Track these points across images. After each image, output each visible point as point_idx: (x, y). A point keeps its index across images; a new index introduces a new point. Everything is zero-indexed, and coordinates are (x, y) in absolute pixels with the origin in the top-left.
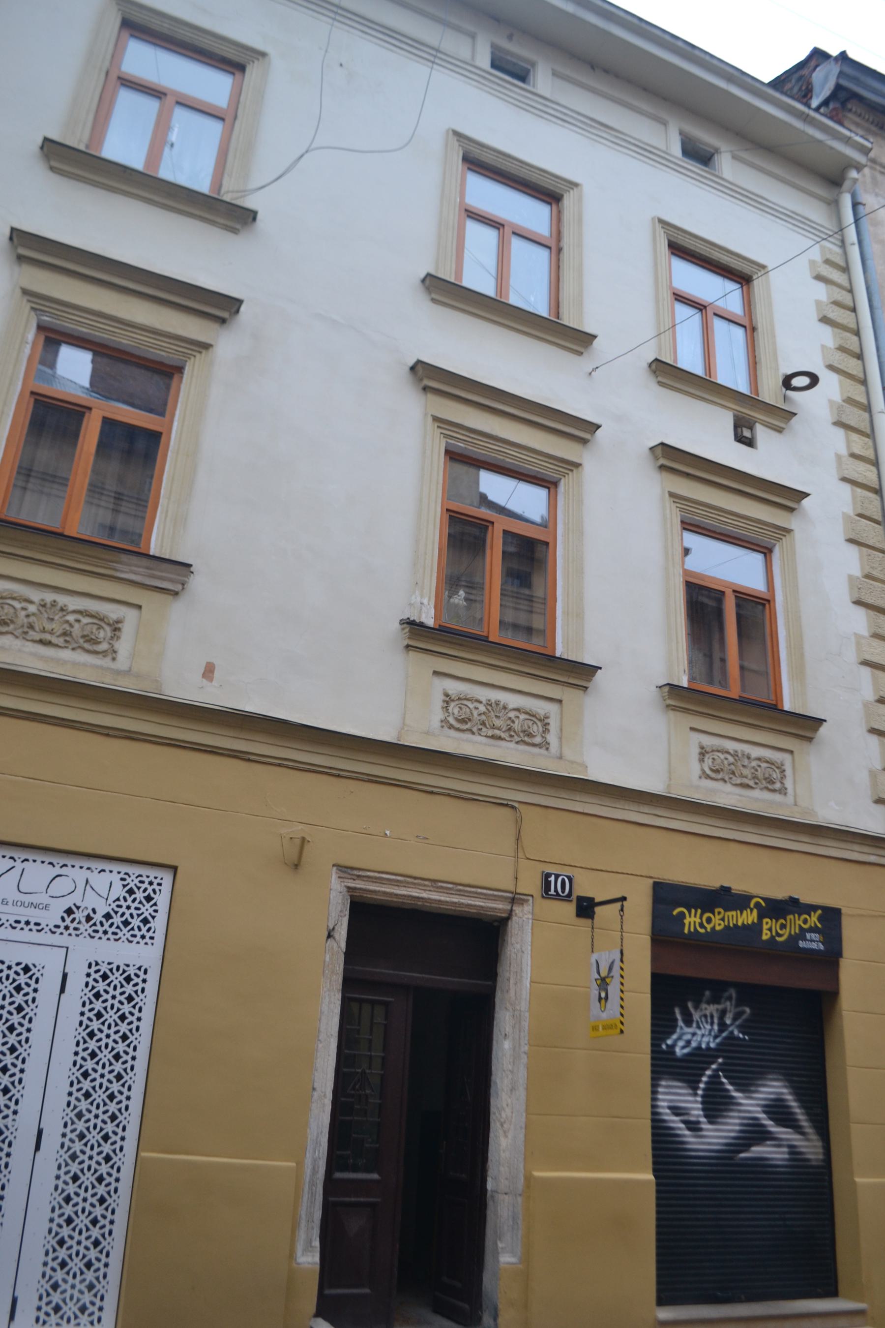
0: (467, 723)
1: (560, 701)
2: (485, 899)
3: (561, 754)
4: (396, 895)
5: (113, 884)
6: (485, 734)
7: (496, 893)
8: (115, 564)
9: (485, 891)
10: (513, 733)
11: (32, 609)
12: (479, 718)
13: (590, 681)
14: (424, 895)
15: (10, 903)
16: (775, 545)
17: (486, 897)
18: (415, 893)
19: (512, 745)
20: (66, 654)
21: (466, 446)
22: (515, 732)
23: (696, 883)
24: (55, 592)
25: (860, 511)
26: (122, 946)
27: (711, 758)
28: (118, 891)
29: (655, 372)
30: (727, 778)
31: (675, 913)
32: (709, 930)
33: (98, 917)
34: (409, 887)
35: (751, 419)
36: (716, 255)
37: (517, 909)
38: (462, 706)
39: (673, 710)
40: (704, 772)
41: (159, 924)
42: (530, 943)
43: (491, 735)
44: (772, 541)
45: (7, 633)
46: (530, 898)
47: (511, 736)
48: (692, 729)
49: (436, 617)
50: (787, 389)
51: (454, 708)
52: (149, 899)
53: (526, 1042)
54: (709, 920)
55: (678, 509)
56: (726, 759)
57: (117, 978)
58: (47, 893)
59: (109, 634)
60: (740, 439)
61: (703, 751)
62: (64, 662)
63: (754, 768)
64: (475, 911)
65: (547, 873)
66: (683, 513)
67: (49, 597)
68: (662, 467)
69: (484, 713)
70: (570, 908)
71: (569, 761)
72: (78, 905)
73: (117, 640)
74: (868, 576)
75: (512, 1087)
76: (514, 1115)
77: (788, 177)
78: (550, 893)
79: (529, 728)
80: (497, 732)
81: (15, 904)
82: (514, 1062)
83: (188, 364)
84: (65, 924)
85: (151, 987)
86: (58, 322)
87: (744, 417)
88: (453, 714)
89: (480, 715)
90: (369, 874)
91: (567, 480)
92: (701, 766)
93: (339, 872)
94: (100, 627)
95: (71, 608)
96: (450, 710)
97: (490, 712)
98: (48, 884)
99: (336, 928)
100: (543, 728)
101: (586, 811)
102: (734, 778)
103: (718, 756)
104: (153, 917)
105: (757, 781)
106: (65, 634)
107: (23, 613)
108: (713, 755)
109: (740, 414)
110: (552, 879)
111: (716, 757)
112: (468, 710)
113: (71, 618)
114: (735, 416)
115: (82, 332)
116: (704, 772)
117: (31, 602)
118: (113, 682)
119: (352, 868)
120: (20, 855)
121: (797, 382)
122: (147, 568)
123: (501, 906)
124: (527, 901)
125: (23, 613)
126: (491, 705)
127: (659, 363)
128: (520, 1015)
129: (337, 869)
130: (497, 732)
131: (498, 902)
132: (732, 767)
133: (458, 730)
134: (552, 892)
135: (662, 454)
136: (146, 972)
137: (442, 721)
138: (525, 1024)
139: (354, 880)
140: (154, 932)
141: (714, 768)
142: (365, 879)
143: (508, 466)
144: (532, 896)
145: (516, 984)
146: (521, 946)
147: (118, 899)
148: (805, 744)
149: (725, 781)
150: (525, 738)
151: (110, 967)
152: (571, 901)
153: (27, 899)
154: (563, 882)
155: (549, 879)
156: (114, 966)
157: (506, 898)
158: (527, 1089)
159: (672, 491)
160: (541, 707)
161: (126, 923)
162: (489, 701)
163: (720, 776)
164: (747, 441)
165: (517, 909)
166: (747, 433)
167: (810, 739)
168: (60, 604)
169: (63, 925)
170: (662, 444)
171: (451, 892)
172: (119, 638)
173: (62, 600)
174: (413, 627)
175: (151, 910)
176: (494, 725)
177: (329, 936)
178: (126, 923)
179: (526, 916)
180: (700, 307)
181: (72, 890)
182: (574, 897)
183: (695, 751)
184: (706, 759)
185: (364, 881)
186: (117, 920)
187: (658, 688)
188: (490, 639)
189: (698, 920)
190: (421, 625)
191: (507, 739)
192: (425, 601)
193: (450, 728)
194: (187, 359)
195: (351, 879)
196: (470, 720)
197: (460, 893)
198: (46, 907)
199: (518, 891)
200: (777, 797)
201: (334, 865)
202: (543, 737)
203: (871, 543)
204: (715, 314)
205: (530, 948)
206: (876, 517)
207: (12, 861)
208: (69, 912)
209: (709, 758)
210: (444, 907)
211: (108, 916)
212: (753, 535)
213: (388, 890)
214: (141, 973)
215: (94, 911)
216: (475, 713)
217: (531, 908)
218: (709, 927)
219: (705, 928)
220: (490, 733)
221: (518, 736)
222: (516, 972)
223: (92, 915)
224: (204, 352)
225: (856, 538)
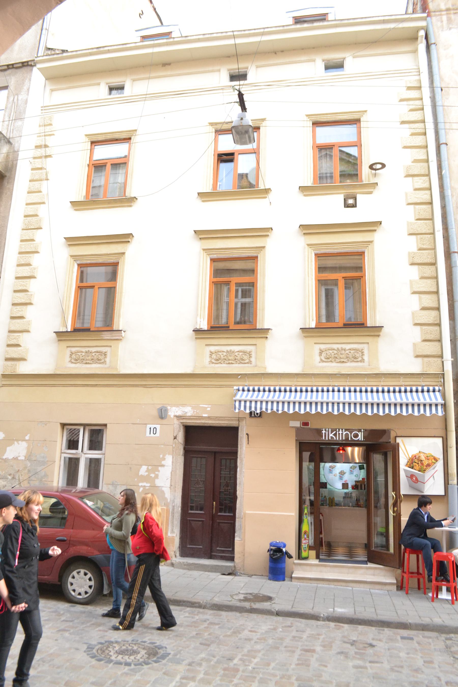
1: (256, 345)
4: (197, 423)
10: (237, 361)
11: (83, 354)
14: (207, 422)
19: (237, 365)
20: (94, 366)
25: (417, 218)
40: (321, 360)
45: (78, 363)
46: (245, 419)
51: (214, 356)
59: (104, 357)
60: (347, 206)
63: (347, 353)
66: (315, 251)
67: (87, 349)
69: (226, 355)
74: (420, 249)
77: (389, 51)
80: (230, 362)
94: (101, 355)
95: (93, 351)
102: (337, 360)
105: (348, 359)
106: (92, 359)
107: (81, 356)
111: (327, 353)
112: (219, 356)
114: (344, 196)
116: (321, 360)
122: (111, 334)
123: (235, 423)
125: (81, 356)
126: (228, 352)
130: (230, 362)
132: (336, 356)
133: (216, 363)
144: (245, 418)
148: (376, 338)
150: (242, 361)
159: (308, 243)
163: (330, 359)
164: (351, 205)
165: (240, 423)
166: (351, 201)
167: (379, 336)
168: (90, 351)
173: (91, 349)
174: (197, 331)
177: (175, 438)
183: (317, 352)
184: (323, 355)
199: (240, 417)
200: (360, 364)
203: (423, 232)
206: (428, 217)
213: (194, 422)
216: (222, 356)
220: (228, 363)
221: (239, 361)
225: (414, 232)
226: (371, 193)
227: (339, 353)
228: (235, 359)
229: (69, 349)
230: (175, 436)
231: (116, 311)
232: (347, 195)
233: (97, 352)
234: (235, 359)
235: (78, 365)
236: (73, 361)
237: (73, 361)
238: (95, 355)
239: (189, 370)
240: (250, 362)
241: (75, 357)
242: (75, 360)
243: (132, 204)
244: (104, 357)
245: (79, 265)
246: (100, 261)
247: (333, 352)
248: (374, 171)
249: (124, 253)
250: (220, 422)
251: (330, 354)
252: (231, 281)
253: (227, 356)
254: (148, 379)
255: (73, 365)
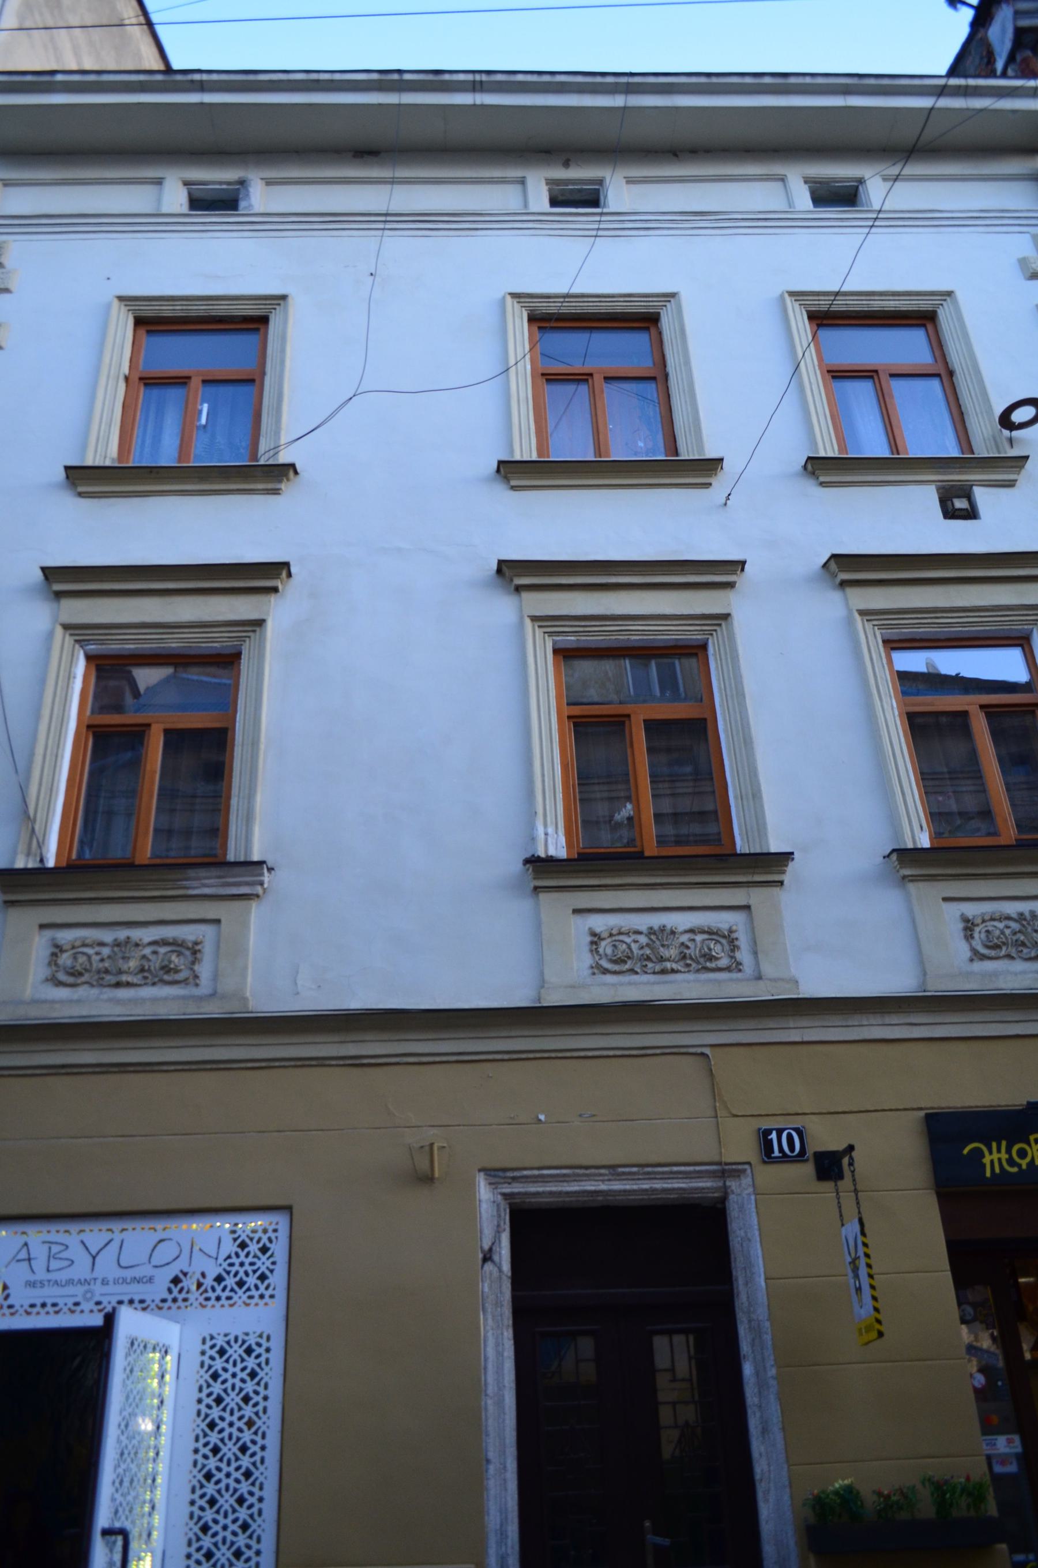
0: (625, 962)
2: (686, 1178)
3: (760, 972)
4: (567, 1193)
5: (222, 1240)
6: (652, 971)
7: (698, 1168)
8: (184, 883)
9: (682, 1168)
10: (689, 962)
11: (106, 951)
12: (641, 952)
13: (784, 872)
14: (603, 1187)
15: (111, 1283)
16: (1032, 630)
17: (687, 1176)
18: (590, 1186)
19: (691, 976)
20: (147, 992)
21: (578, 638)
22: (691, 958)
23: (994, 1104)
24: (129, 928)
26: (239, 1311)
27: (984, 930)
28: (229, 1247)
29: (813, 473)
30: (1013, 952)
31: (965, 1152)
32: (1024, 1167)
33: (209, 1282)
34: (582, 1181)
35: (966, 485)
36: (877, 305)
37: (732, 1184)
38: (614, 943)
39: (912, 881)
40: (975, 952)
41: (278, 1279)
42: (756, 1227)
43: (659, 970)
44: (1026, 627)
46: (747, 1167)
47: (688, 965)
48: (945, 899)
49: (569, 844)
50: (1011, 431)
52: (264, 1250)
53: (773, 1363)
54: (1022, 1154)
55: (876, 628)
56: (1008, 927)
57: (235, 1351)
58: (150, 1262)
60: (950, 513)
61: (970, 925)
62: (143, 1001)
64: (676, 1196)
65: (765, 1129)
67: (122, 934)
68: (844, 584)
69: (648, 945)
70: (808, 1169)
71: (770, 980)
72: (185, 1270)
73: (199, 963)
75: (763, 1428)
76: (772, 1468)
78: (773, 1155)
79: (710, 949)
81: (116, 1282)
82: (760, 1392)
83: (243, 647)
84: (172, 1296)
85: (277, 1357)
86: (104, 647)
87: (952, 486)
88: (606, 955)
89: (642, 948)
90: (525, 1173)
91: (715, 638)
92: (971, 945)
93: (488, 1177)
95: (147, 940)
96: (601, 950)
97: (654, 942)
98: (149, 1251)
99: (494, 1248)
100: (730, 945)
101: (806, 1039)
102: (1025, 951)
103: (995, 927)
104: (272, 1271)
106: (142, 970)
108: (986, 926)
109: (944, 483)
110: (774, 1136)
111: (990, 929)
113: (147, 951)
115: (129, 649)
117: (102, 944)
118: (196, 1010)
119: (505, 1170)
120: (117, 1225)
121: (1019, 416)
123: (709, 1184)
124: (745, 1171)
125: (98, 958)
126: (655, 933)
127: (816, 461)
128: (759, 1325)
129: (486, 1174)
131: (705, 1180)
133: (615, 973)
134: (777, 1153)
135: (838, 568)
136: (268, 1339)
137: (592, 967)
138: (768, 1338)
139: (509, 1183)
140: (274, 1289)
141: (990, 944)
142: (523, 1180)
143: (636, 645)
144: (749, 1163)
145: (746, 1284)
146: (746, 1232)
147: (229, 1257)
149: (1013, 958)
150: (705, 962)
151: (227, 1339)
152: (807, 1160)
153: (129, 1274)
154: (790, 1138)
155: (769, 1137)
156: (232, 1338)
157: (714, 1172)
158: (783, 1429)
160: (722, 920)
161: (241, 1284)
162: (651, 928)
164: (962, 513)
165: (732, 1184)
166: (960, 504)
169: (170, 1297)
170: (834, 556)
171: (637, 1177)
172: (200, 961)
175: (268, 1263)
176: (662, 957)
178: (241, 1284)
179: (746, 1192)
180: (869, 374)
181: (177, 1253)
182: (809, 1153)
184: (976, 935)
185: (521, 1182)
186: (230, 1281)
187: (886, 859)
188: (647, 854)
189: (1004, 1156)
190: (550, 860)
191: (683, 970)
192: (551, 830)
193: (604, 973)
194: (242, 643)
195: (505, 1183)
196: (629, 958)
197: (650, 1177)
198: (151, 1280)
201: (480, 1170)
202: (732, 957)
204: (892, 375)
205: (757, 1233)
207: (110, 1233)
208: (176, 1281)
209: (980, 932)
210: (633, 1197)
211: (219, 1279)
212: (993, 628)
213: (554, 1189)
214: (263, 1341)
215: (203, 1275)
216: (634, 946)
217: (749, 1180)
218: (1024, 1163)
219: (1019, 1166)
220: (658, 968)
221: (698, 963)
222: (745, 1268)
223: (202, 1280)
224: (258, 629)
226: (1010, 484)
227: (1029, 929)
228: (684, 957)
229: (48, 934)
230: (486, 1247)
231: (234, 802)
232: (943, 488)
233: (164, 942)
234: (684, 957)
235: (82, 992)
236: (62, 976)
237: (62, 976)
238: (155, 953)
239: (520, 998)
240: (736, 966)
241: (69, 962)
242: (72, 974)
243: (283, 486)
244: (190, 958)
245: (89, 658)
246: (174, 645)
247: (1008, 927)
248: (1006, 433)
249: (260, 623)
250: (658, 1185)
251: (997, 933)
252: (628, 716)
253: (652, 949)
254: (368, 1036)
255: (63, 993)
